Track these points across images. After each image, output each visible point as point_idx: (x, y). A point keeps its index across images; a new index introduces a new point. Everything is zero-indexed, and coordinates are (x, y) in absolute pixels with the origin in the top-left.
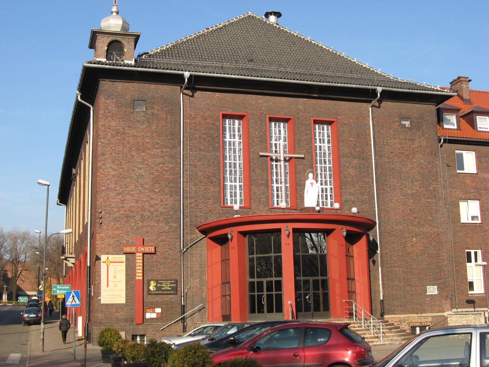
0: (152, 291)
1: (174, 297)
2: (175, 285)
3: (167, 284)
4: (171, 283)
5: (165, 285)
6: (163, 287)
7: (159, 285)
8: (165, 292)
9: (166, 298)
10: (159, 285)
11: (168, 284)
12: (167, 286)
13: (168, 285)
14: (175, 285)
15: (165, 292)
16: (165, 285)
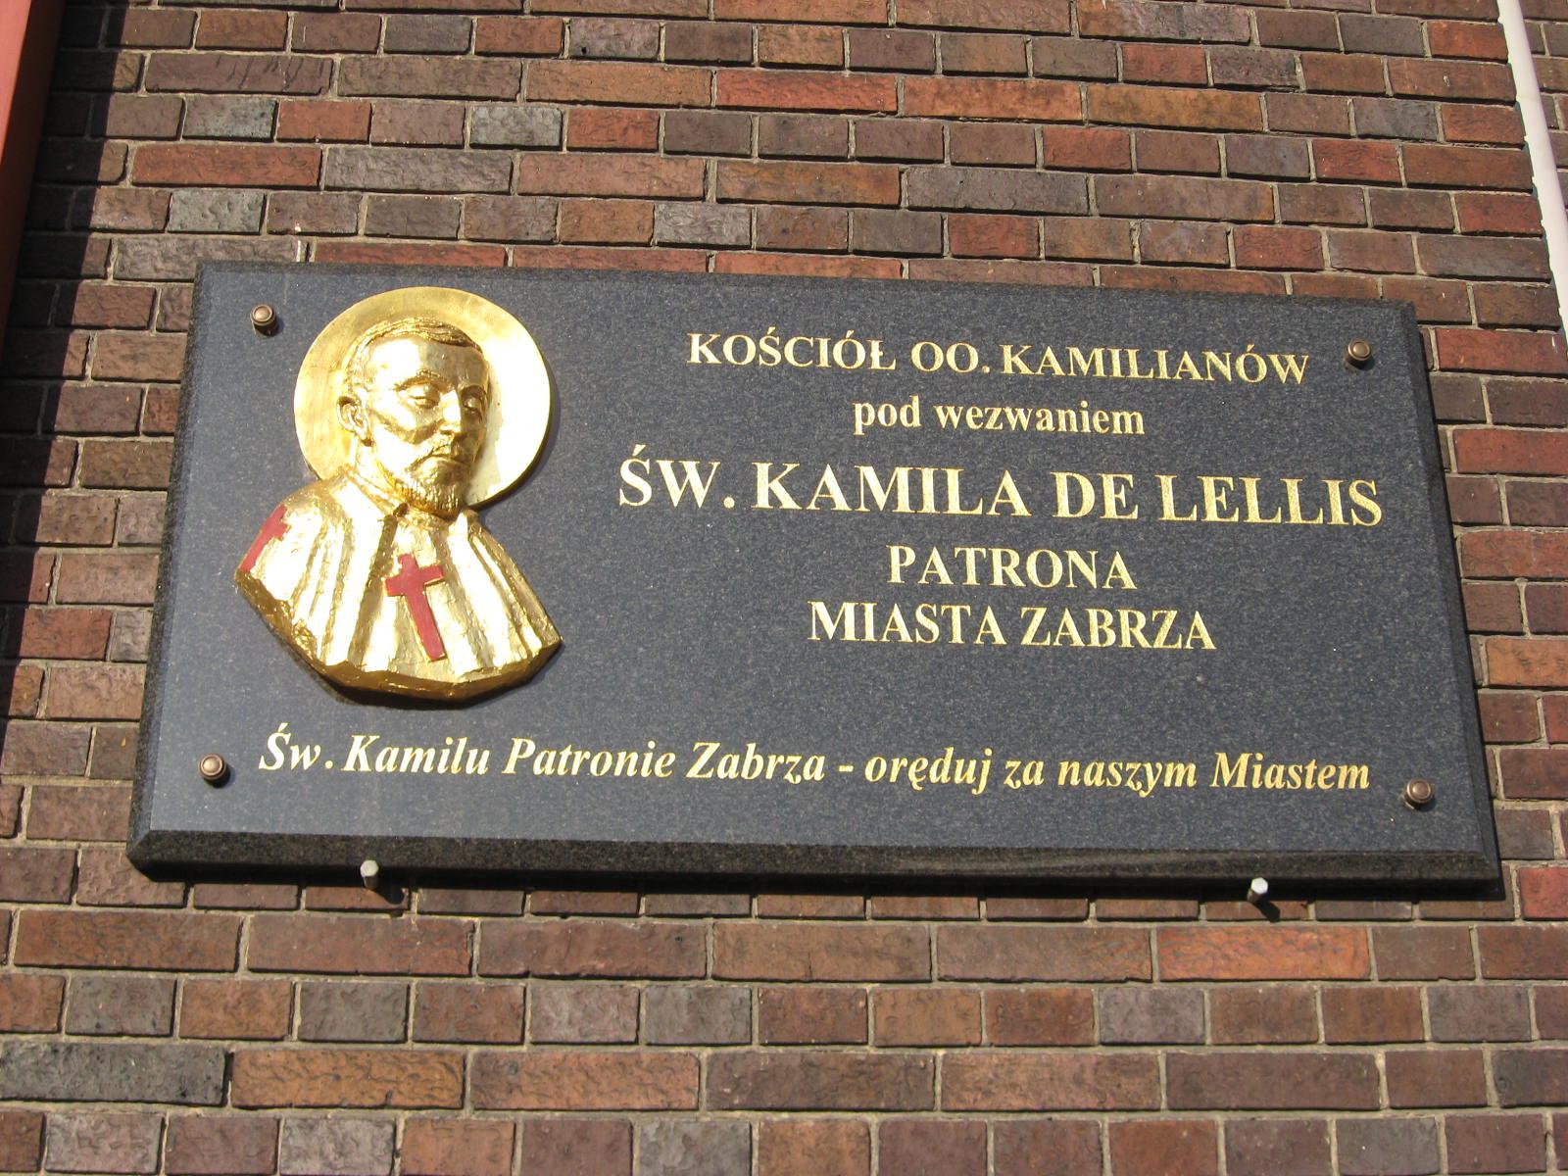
0: (358, 692)
1: (1384, 1018)
2: (1353, 502)
3: (1038, 460)
4: (1195, 431)
5: (945, 490)
6: (849, 553)
7: (689, 482)
8: (947, 769)
9: (1023, 1025)
10: (689, 482)
11: (1088, 455)
12: (1039, 531)
13: (1108, 495)
14: (1353, 502)
15: (947, 769)
16: (945, 490)
